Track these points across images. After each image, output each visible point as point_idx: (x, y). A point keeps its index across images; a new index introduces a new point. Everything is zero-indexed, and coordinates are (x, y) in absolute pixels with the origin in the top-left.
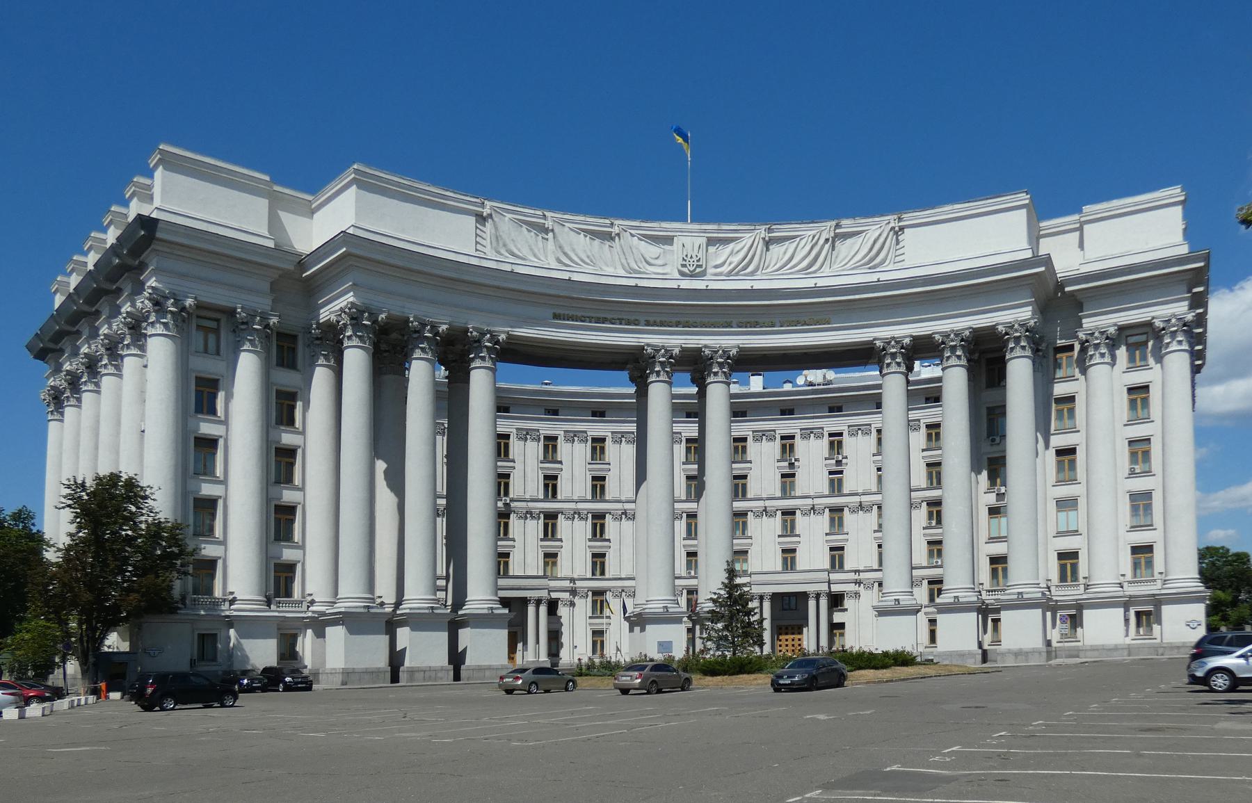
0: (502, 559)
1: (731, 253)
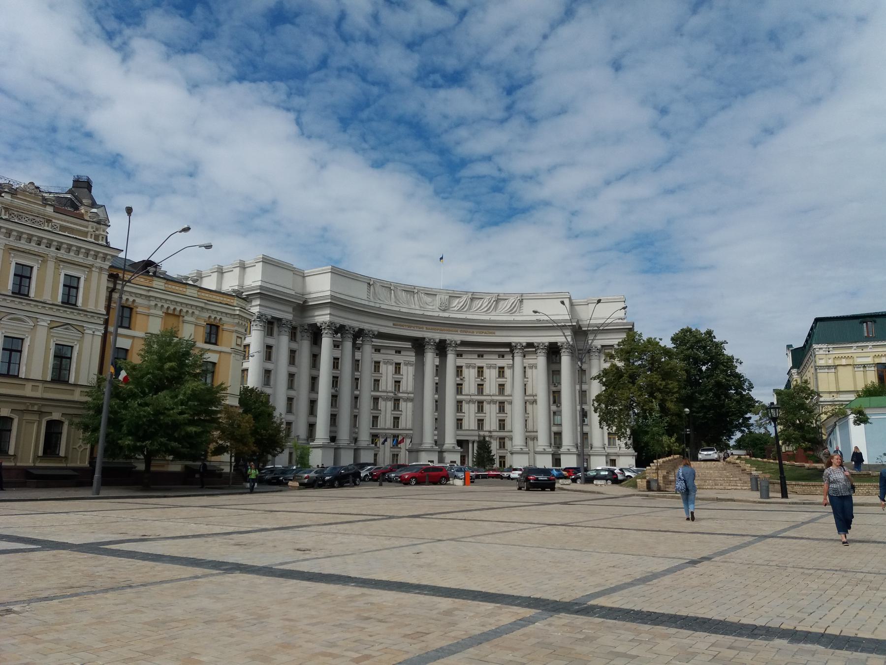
0: (459, 423)
1: (459, 303)
